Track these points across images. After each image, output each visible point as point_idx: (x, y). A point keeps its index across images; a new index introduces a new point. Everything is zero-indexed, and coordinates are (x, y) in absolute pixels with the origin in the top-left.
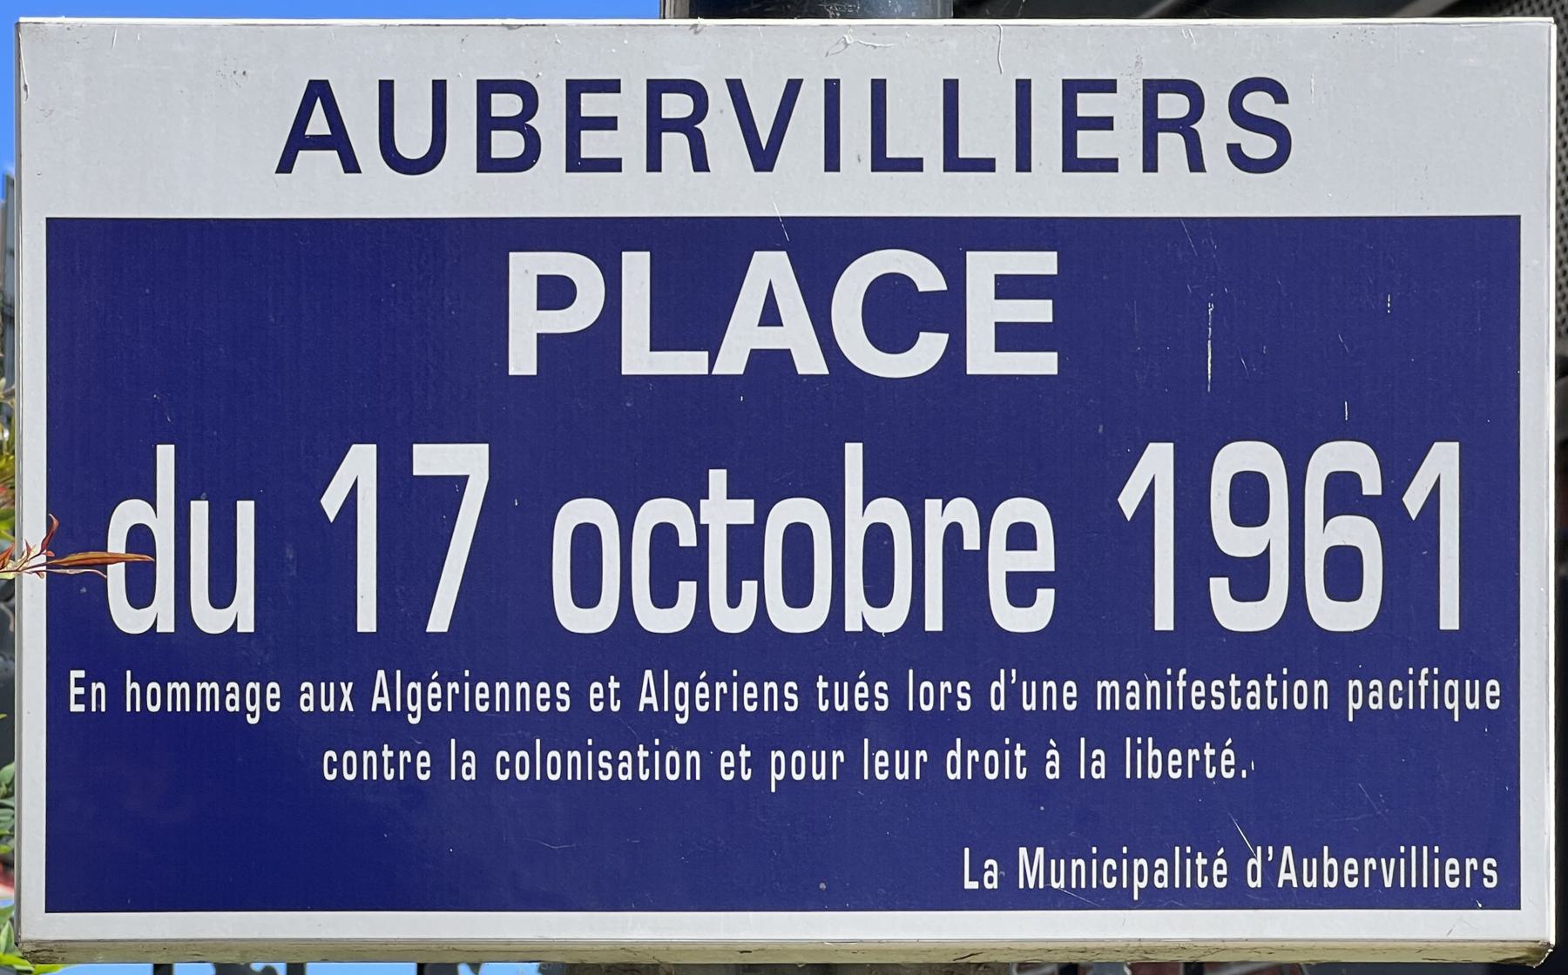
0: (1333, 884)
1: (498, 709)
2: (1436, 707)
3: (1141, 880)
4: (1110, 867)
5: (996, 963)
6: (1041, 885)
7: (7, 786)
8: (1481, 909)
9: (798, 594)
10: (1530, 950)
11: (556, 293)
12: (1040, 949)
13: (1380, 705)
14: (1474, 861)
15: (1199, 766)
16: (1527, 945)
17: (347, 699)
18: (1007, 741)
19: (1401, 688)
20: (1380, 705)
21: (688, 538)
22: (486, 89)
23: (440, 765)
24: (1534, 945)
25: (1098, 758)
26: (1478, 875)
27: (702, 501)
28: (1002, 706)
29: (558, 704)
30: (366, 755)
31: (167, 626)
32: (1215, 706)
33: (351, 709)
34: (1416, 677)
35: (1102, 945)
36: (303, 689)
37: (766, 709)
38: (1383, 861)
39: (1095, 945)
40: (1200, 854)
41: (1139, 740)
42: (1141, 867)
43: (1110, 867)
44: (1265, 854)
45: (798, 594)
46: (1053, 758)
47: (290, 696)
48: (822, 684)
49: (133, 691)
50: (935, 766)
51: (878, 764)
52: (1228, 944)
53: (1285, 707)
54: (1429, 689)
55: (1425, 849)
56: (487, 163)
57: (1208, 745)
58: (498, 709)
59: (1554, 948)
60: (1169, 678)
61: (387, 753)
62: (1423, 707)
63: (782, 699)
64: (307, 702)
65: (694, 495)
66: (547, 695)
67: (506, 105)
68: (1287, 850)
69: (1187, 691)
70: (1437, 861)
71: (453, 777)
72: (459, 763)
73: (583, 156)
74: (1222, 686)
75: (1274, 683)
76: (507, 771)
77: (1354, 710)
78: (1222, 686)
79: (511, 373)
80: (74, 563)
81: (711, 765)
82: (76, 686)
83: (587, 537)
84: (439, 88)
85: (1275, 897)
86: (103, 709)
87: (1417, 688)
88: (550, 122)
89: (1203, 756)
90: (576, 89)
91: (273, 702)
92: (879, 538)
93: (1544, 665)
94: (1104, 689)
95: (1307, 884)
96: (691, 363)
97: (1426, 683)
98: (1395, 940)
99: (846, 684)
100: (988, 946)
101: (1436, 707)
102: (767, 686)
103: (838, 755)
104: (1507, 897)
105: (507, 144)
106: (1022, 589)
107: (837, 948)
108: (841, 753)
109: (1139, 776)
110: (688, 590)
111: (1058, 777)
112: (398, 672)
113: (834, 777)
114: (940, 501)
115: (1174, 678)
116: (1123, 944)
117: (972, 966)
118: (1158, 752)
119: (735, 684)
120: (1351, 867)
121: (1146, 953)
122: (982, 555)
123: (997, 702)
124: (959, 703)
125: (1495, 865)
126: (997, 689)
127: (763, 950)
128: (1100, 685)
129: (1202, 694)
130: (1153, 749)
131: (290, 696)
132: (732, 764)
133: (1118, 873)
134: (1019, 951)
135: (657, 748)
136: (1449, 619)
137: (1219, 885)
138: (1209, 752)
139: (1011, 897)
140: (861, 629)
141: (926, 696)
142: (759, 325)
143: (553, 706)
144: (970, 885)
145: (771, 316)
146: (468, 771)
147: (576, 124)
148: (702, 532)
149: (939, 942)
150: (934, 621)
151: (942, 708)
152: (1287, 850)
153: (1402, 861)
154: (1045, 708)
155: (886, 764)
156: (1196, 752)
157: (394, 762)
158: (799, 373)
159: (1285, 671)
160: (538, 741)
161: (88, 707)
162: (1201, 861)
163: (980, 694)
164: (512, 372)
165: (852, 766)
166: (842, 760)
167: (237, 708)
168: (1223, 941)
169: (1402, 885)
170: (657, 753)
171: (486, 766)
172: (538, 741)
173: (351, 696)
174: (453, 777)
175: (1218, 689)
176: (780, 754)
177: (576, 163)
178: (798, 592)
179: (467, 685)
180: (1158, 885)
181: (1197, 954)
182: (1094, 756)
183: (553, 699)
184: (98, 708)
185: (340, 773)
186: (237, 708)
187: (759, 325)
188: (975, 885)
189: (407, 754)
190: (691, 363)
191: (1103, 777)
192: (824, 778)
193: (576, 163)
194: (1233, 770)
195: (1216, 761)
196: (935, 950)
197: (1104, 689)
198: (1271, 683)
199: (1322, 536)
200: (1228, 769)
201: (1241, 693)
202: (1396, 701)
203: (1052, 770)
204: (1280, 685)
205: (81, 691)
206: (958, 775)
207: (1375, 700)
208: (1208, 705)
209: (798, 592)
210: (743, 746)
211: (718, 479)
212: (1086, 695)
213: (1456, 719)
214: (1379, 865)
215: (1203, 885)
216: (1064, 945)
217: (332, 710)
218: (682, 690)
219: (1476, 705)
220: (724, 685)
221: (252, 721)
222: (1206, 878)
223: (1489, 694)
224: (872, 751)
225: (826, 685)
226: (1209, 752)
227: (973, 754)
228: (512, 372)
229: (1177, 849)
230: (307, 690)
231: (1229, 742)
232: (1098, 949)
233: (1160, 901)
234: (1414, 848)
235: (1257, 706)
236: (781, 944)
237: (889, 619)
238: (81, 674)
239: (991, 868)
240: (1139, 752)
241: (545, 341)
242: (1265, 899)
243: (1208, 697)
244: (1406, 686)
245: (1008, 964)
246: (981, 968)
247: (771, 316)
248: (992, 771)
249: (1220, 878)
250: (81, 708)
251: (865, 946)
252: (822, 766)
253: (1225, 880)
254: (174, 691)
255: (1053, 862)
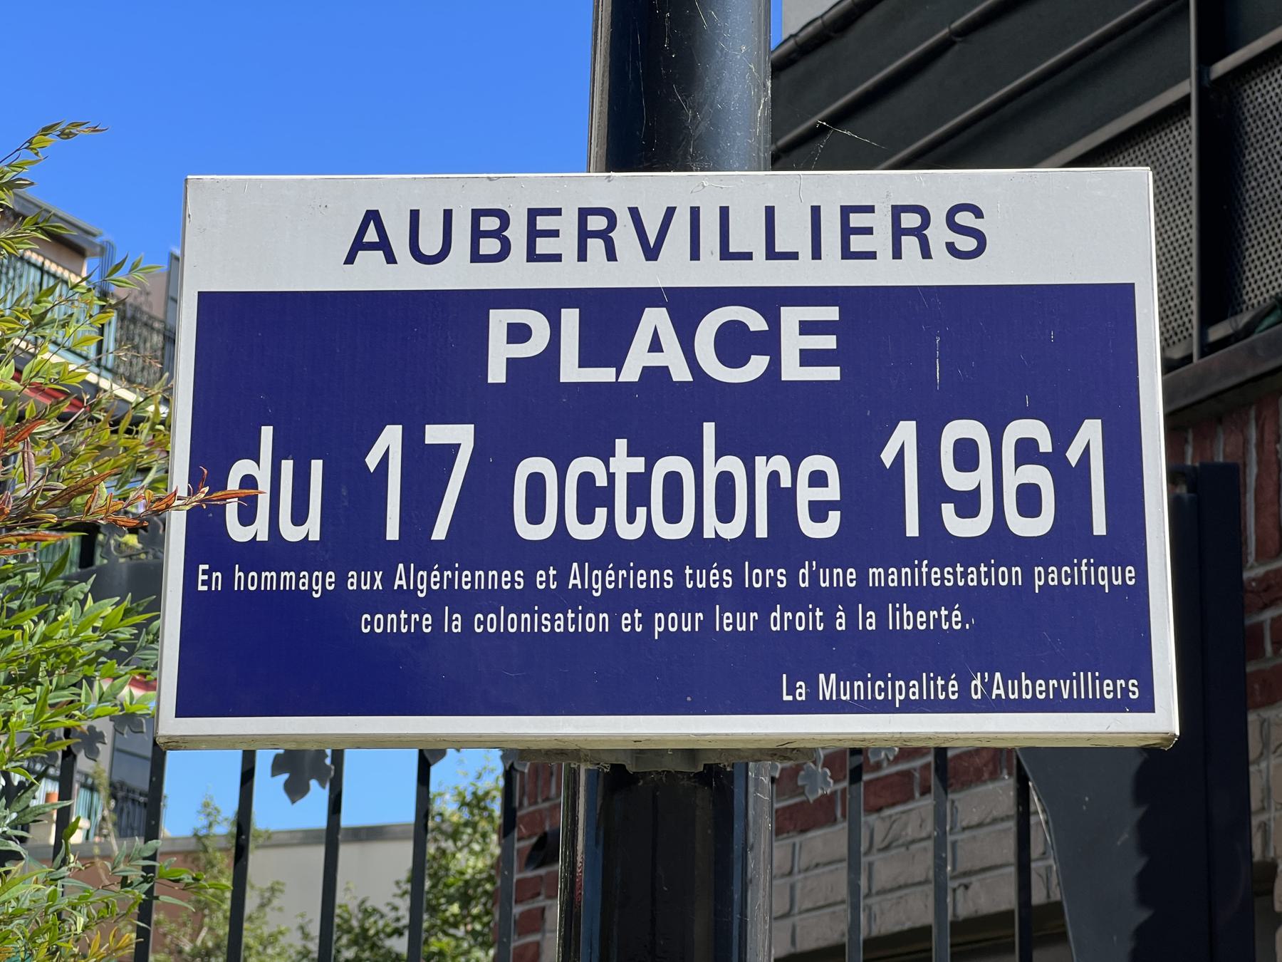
0: (1029, 697)
1: (476, 587)
2: (1093, 583)
3: (900, 694)
4: (880, 686)
5: (805, 748)
6: (834, 698)
7: (154, 635)
8: (1128, 712)
9: (673, 515)
10: (1162, 739)
11: (519, 333)
12: (834, 739)
13: (1056, 583)
14: (1122, 681)
15: (938, 621)
16: (1161, 735)
17: (378, 582)
18: (810, 606)
19: (1069, 572)
20: (1056, 583)
21: (601, 481)
22: (477, 214)
23: (437, 623)
24: (1165, 736)
25: (871, 617)
26: (1125, 690)
27: (611, 459)
28: (807, 584)
29: (516, 584)
30: (390, 617)
31: (263, 536)
32: (947, 584)
33: (381, 588)
34: (1079, 565)
35: (876, 736)
36: (350, 576)
37: (652, 587)
38: (1062, 681)
39: (870, 736)
40: (939, 678)
41: (898, 605)
42: (900, 686)
43: (880, 686)
44: (983, 678)
45: (673, 515)
46: (841, 617)
47: (341, 580)
48: (688, 571)
49: (240, 577)
50: (763, 622)
51: (725, 621)
52: (960, 735)
53: (993, 584)
54: (1088, 573)
55: (1089, 674)
56: (476, 257)
57: (943, 608)
58: (476, 587)
59: (1179, 738)
60: (1076, 565)
61: (403, 616)
62: (1084, 583)
63: (662, 580)
64: (352, 584)
65: (606, 454)
66: (509, 579)
67: (489, 223)
68: (998, 675)
69: (929, 574)
70: (1097, 681)
71: (446, 631)
72: (450, 621)
73: (537, 253)
74: (951, 571)
75: (986, 569)
76: (482, 626)
77: (1039, 585)
78: (951, 571)
79: (489, 382)
80: (219, 498)
81: (615, 622)
82: (202, 574)
83: (536, 482)
84: (448, 215)
85: (990, 705)
86: (219, 589)
87: (1080, 572)
88: (517, 233)
89: (940, 615)
90: (533, 214)
91: (330, 584)
92: (725, 481)
93: (1163, 556)
94: (874, 573)
95: (1012, 697)
96: (605, 375)
97: (927, 570)
98: (1071, 733)
99: (704, 571)
100: (799, 737)
101: (1093, 583)
102: (652, 573)
103: (699, 615)
104: (1146, 704)
105: (490, 246)
106: (819, 511)
107: (699, 739)
108: (701, 615)
109: (898, 628)
110: (601, 513)
111: (844, 629)
112: (412, 565)
113: (697, 630)
114: (765, 458)
115: (920, 566)
116: (889, 736)
117: (789, 750)
118: (910, 613)
119: (632, 572)
120: (1040, 685)
121: (905, 741)
122: (792, 491)
123: (804, 582)
124: (779, 583)
125: (1136, 684)
126: (804, 574)
127: (649, 740)
128: (871, 571)
129: (939, 576)
130: (907, 611)
131: (341, 580)
132: (630, 621)
133: (885, 690)
134: (820, 740)
135: (580, 612)
136: (1100, 528)
137: (952, 697)
138: (944, 612)
139: (813, 705)
140: (714, 537)
141: (756, 578)
142: (649, 352)
143: (513, 586)
144: (787, 698)
145: (656, 346)
146: (456, 627)
147: (534, 234)
148: (611, 477)
149: (766, 734)
150: (762, 531)
151: (767, 586)
152: (998, 675)
153: (1075, 681)
154: (835, 585)
155: (731, 621)
156: (935, 613)
157: (408, 621)
158: (674, 380)
159: (993, 562)
160: (502, 608)
161: (210, 587)
162: (940, 682)
163: (792, 577)
164: (490, 381)
165: (708, 623)
166: (702, 619)
167: (306, 587)
168: (956, 733)
169: (1075, 697)
170: (580, 615)
171: (467, 624)
172: (502, 608)
173: (381, 580)
174: (446, 631)
175: (949, 573)
176: (661, 615)
177: (532, 256)
178: (673, 513)
179: (457, 572)
180: (912, 697)
181: (939, 742)
182: (868, 616)
183: (513, 581)
184: (216, 588)
185: (372, 628)
186: (306, 587)
187: (649, 352)
188: (790, 698)
189: (417, 616)
190: (605, 375)
191: (874, 629)
192: (690, 630)
193: (532, 256)
194: (960, 624)
195: (948, 618)
196: (764, 740)
197: (874, 573)
198: (983, 569)
199: (1014, 477)
200: (957, 623)
201: (965, 575)
202: (1066, 580)
203: (841, 624)
204: (989, 570)
205: (206, 577)
206: (778, 628)
207: (1053, 580)
208: (942, 583)
209: (673, 513)
210: (637, 610)
211: (621, 445)
212: (862, 577)
213: (1107, 591)
214: (1059, 684)
215: (942, 697)
216: (850, 737)
217: (369, 588)
218: (597, 575)
219: (1120, 582)
220: (624, 572)
221: (316, 596)
222: (944, 693)
223: (1128, 575)
224: (722, 613)
225: (691, 571)
226: (944, 612)
227: (788, 615)
228: (490, 381)
229: (924, 674)
230: (352, 576)
231: (957, 606)
232: (872, 739)
233: (914, 708)
234: (1082, 674)
235: (975, 583)
236: (661, 736)
237: (732, 530)
238: (206, 567)
239: (801, 687)
240: (898, 613)
241: (511, 363)
242: (984, 706)
243: (943, 578)
244: (1072, 570)
245: (814, 748)
246: (795, 752)
247: (656, 346)
248: (800, 625)
249: (953, 693)
250: (205, 588)
251: (718, 737)
252: (689, 623)
253: (957, 694)
254: (266, 577)
255: (842, 683)
